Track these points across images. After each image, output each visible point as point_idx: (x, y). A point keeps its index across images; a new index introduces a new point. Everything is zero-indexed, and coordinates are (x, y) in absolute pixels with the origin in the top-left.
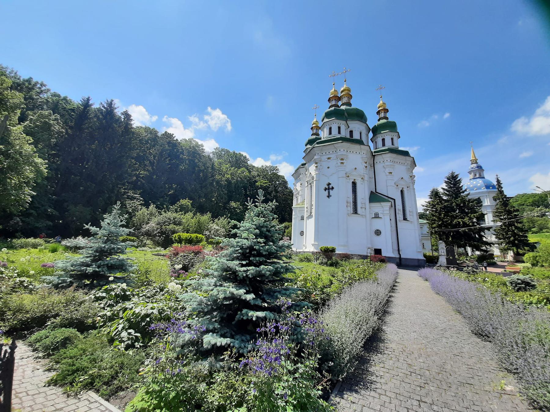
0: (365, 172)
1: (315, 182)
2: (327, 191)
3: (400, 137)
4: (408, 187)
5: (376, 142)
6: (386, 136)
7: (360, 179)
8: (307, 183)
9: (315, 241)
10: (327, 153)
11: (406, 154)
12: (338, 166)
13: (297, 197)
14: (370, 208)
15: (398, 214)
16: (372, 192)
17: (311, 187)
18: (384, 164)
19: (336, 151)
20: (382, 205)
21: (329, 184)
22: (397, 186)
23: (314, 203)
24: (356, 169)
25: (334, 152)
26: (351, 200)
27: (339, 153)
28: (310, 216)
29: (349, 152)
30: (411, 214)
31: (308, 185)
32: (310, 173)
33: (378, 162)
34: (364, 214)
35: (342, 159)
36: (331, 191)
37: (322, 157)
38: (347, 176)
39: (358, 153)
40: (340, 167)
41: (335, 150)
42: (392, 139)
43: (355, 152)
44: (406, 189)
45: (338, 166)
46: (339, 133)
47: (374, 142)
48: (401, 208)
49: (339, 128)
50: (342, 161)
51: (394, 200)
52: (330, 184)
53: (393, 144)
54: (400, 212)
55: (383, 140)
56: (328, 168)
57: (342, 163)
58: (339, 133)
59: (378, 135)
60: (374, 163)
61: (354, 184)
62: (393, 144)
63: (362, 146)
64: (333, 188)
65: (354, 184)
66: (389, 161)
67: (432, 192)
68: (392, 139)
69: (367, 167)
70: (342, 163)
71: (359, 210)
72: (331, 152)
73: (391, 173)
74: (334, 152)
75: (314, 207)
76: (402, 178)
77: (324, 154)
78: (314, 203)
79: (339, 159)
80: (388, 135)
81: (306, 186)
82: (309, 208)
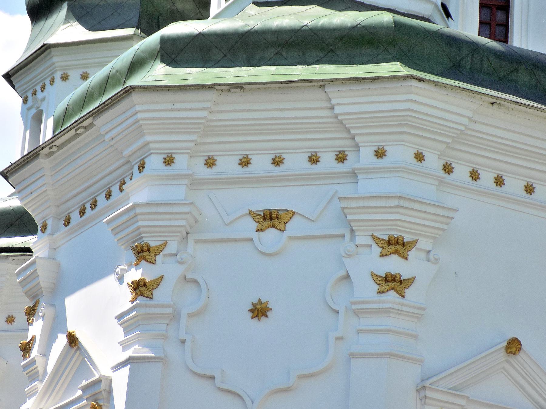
19: (341, 158)
32: (72, 340)
40: (367, 322)
41: (344, 144)
79: (363, 239)
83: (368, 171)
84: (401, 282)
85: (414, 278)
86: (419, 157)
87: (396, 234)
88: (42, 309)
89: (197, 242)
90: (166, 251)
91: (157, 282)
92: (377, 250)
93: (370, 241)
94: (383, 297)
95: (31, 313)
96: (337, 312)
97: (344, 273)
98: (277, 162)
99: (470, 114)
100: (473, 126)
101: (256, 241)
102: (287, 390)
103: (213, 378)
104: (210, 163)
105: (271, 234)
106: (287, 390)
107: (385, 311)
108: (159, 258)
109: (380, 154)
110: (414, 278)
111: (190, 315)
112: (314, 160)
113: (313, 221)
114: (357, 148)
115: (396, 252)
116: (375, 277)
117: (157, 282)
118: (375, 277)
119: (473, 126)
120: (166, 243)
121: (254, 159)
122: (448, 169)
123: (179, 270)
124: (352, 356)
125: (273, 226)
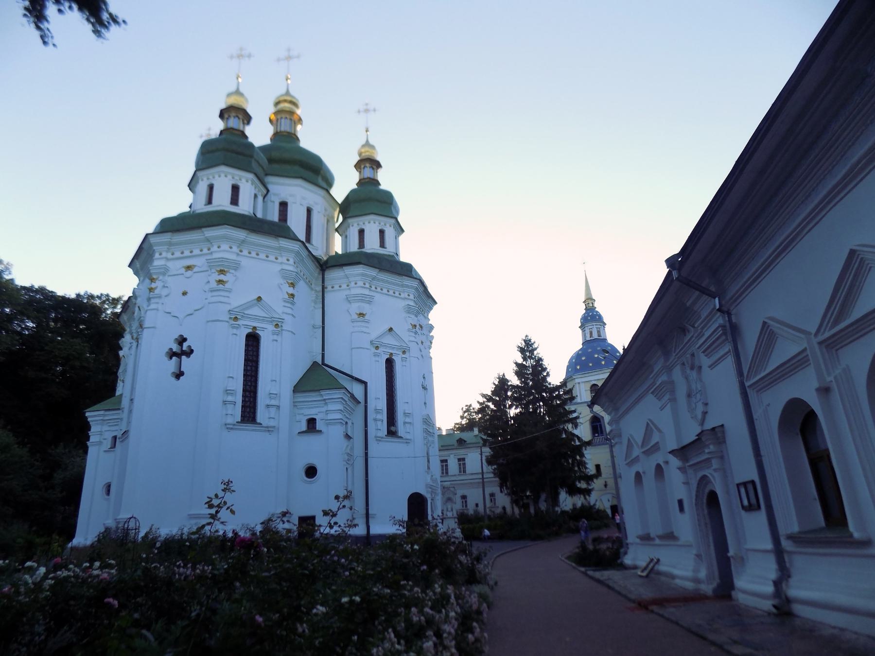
0: (289, 311)
2: (174, 358)
3: (402, 231)
4: (404, 352)
5: (346, 237)
6: (366, 223)
7: (271, 327)
10: (187, 253)
11: (406, 270)
12: (212, 291)
14: (295, 406)
16: (315, 364)
18: (347, 292)
19: (209, 249)
20: (324, 398)
21: (182, 340)
22: (377, 348)
24: (259, 299)
25: (205, 251)
26: (238, 385)
27: (215, 256)
29: (245, 252)
30: (408, 420)
33: (336, 287)
34: (272, 423)
35: (222, 272)
36: (184, 357)
37: (170, 264)
38: (233, 317)
39: (272, 258)
42: (382, 232)
43: (262, 256)
44: (400, 357)
45: (212, 291)
46: (235, 201)
47: (344, 237)
48: (383, 404)
49: (235, 189)
50: (222, 277)
51: (365, 383)
52: (185, 340)
53: (382, 244)
55: (361, 232)
56: (185, 294)
57: (220, 282)
58: (235, 201)
59: (350, 221)
60: (323, 288)
61: (253, 341)
62: (382, 244)
63: (284, 243)
64: (189, 353)
65: (253, 341)
66: (360, 284)
68: (382, 232)
69: (292, 296)
70: (220, 282)
71: (261, 414)
72: (196, 252)
73: (361, 315)
74: (205, 251)
76: (391, 329)
77: (178, 254)
80: (372, 222)
83: (216, 252)
84: (223, 281)
85: (228, 281)
86: (231, 248)
87: (222, 269)
89: (169, 276)
90: (159, 279)
91: (156, 288)
92: (217, 273)
93: (215, 271)
94: (219, 286)
96: (205, 291)
97: (207, 281)
98: (191, 252)
99: (246, 235)
100: (247, 238)
101: (185, 274)
102: (191, 314)
103: (170, 313)
104: (173, 254)
105: (190, 271)
106: (191, 314)
107: (220, 290)
108: (157, 281)
109: (219, 247)
110: (228, 281)
111: (166, 296)
112: (201, 251)
113: (200, 267)
114: (213, 246)
115: (222, 274)
116: (216, 281)
117: (156, 288)
118: (216, 281)
119: (247, 238)
120: (159, 277)
121: (185, 252)
122: (241, 251)
123: (162, 284)
124: (209, 303)
125: (189, 270)
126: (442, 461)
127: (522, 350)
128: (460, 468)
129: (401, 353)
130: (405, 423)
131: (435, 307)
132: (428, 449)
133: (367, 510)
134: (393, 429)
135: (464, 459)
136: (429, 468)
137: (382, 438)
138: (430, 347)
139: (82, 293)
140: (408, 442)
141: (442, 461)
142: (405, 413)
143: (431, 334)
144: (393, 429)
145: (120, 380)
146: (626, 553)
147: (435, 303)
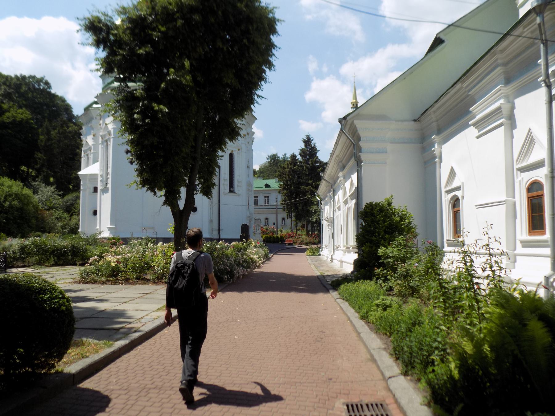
1: (112, 140)
8: (102, 138)
9: (111, 224)
13: (87, 155)
15: (224, 184)
17: (107, 145)
23: (110, 170)
28: (105, 190)
30: (239, 184)
31: (102, 143)
48: (228, 177)
54: (226, 183)
67: (274, 155)
75: (110, 176)
78: (110, 170)
81: (100, 142)
82: (104, 176)
88: (102, 119)
95: (100, 119)
126: (255, 197)
127: (305, 142)
128: (265, 202)
129: (237, 150)
130: (238, 186)
131: (256, 121)
132: (249, 198)
133: (219, 227)
134: (232, 189)
135: (268, 197)
136: (248, 208)
137: (227, 193)
138: (252, 144)
139: (19, 75)
140: (239, 195)
141: (255, 197)
142: (238, 181)
143: (253, 137)
144: (232, 189)
145: (84, 153)
146: (322, 251)
147: (257, 119)
